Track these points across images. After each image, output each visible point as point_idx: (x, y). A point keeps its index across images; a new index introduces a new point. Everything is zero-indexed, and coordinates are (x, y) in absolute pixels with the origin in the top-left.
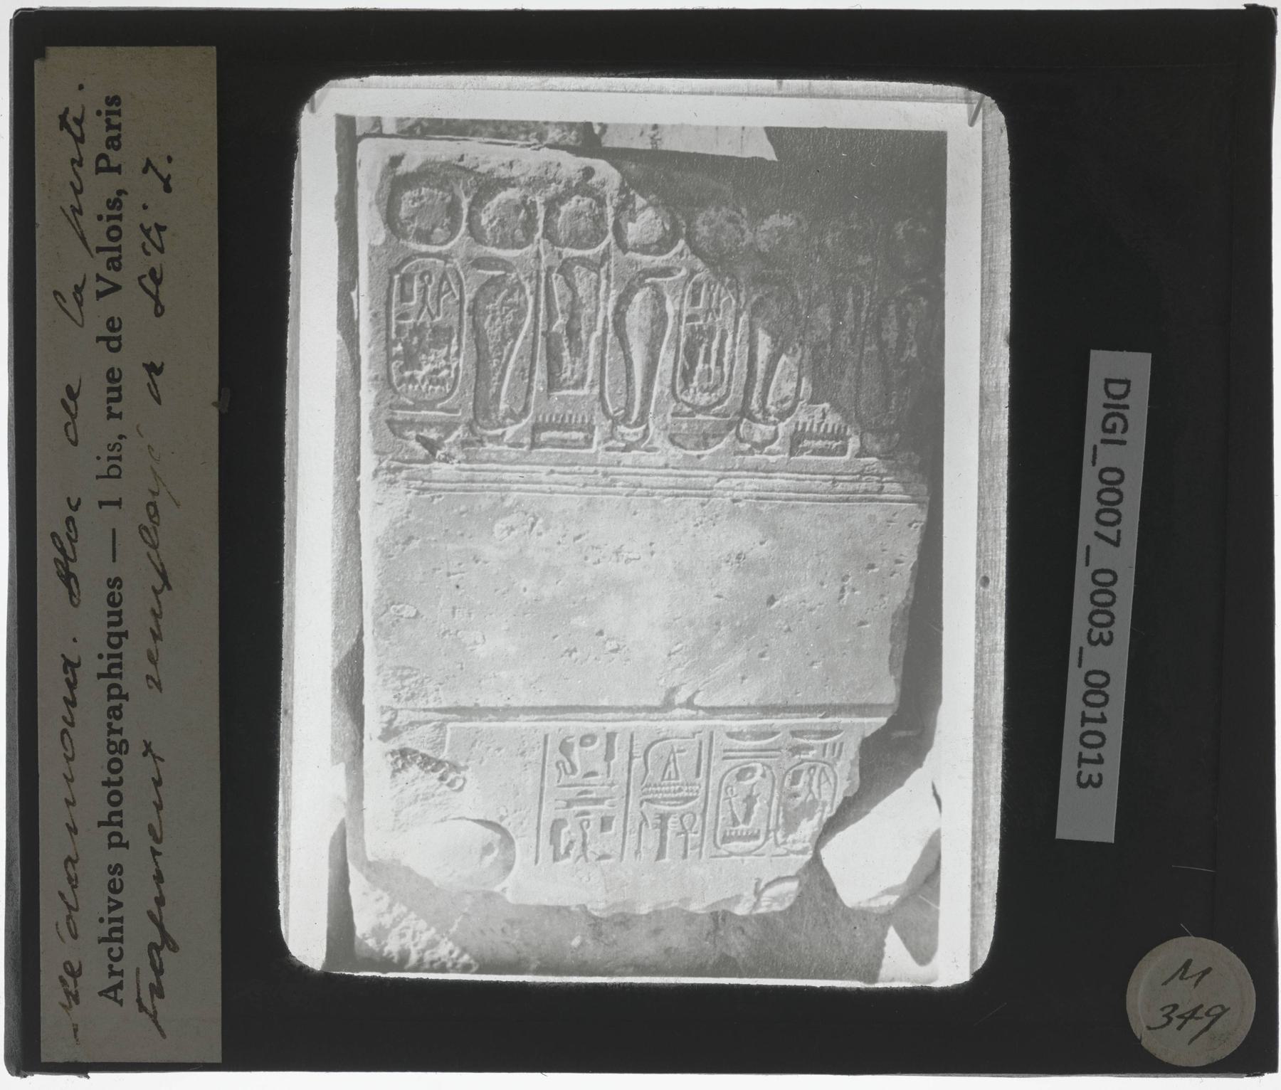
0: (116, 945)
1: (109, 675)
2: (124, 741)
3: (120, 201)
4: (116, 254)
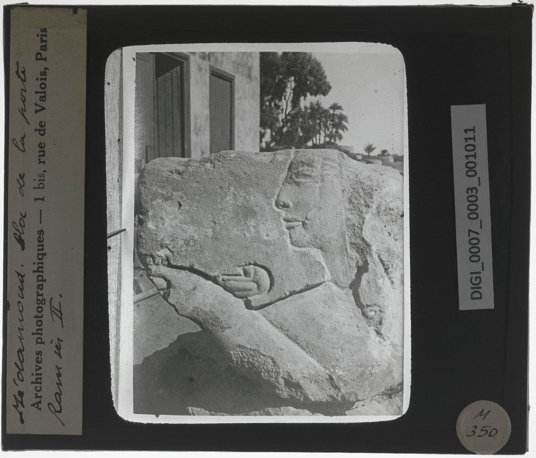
0: (38, 385)
1: (38, 271)
2: (44, 299)
3: (46, 72)
4: (43, 95)
